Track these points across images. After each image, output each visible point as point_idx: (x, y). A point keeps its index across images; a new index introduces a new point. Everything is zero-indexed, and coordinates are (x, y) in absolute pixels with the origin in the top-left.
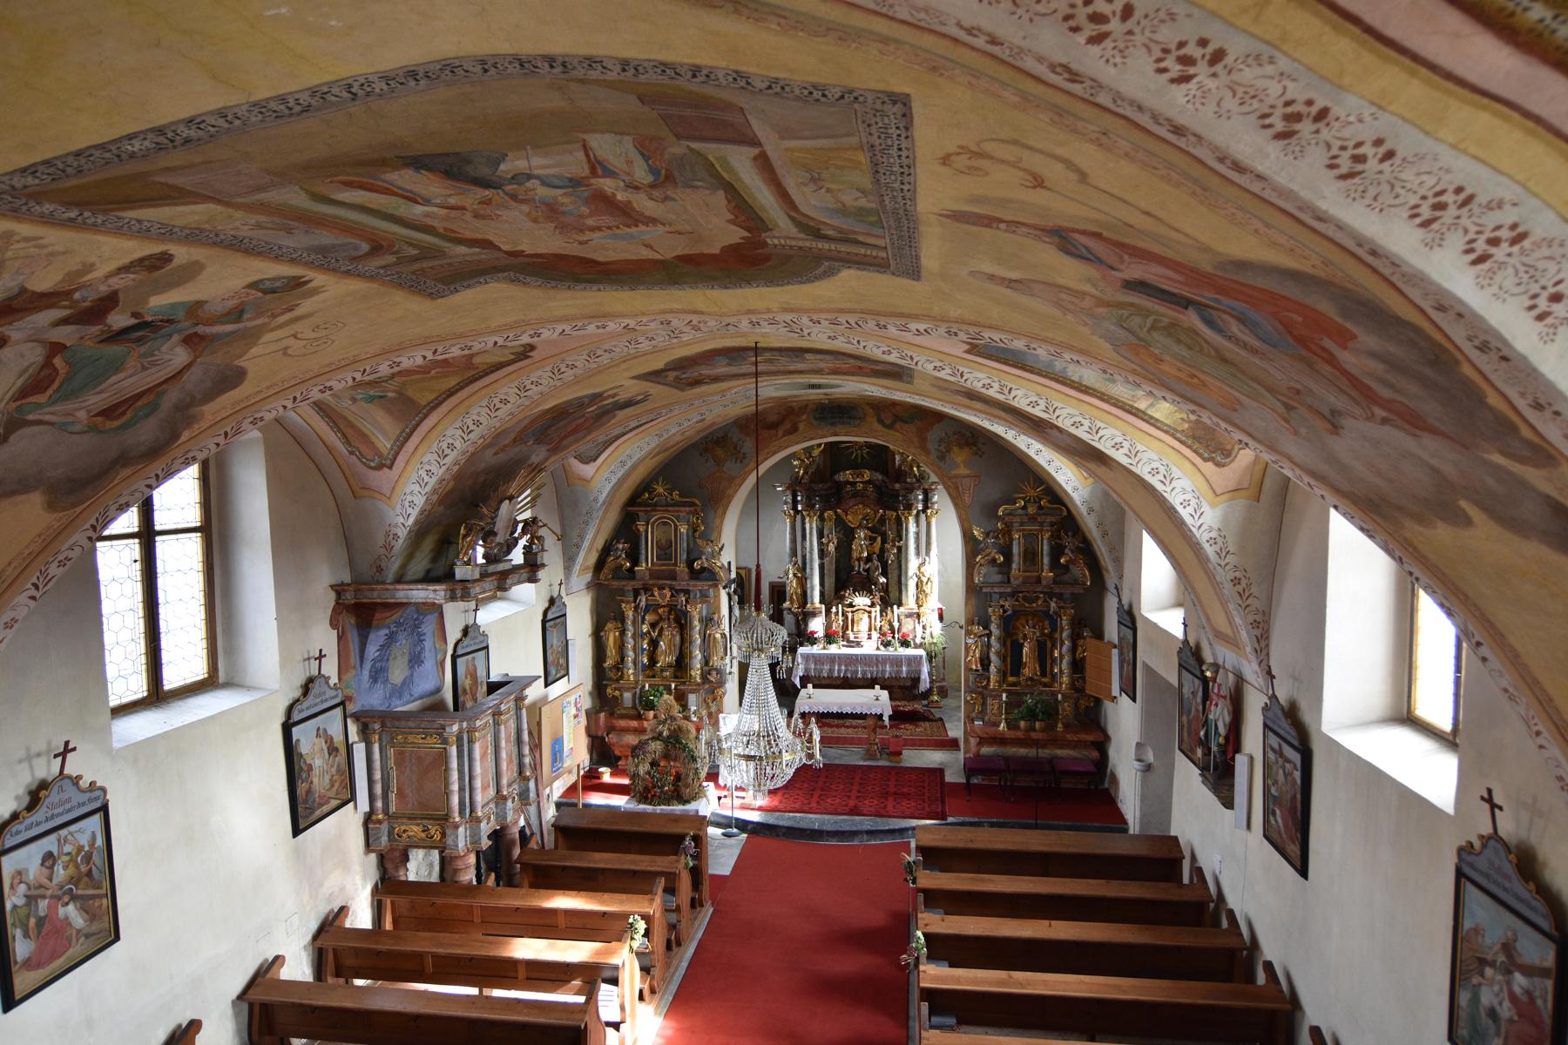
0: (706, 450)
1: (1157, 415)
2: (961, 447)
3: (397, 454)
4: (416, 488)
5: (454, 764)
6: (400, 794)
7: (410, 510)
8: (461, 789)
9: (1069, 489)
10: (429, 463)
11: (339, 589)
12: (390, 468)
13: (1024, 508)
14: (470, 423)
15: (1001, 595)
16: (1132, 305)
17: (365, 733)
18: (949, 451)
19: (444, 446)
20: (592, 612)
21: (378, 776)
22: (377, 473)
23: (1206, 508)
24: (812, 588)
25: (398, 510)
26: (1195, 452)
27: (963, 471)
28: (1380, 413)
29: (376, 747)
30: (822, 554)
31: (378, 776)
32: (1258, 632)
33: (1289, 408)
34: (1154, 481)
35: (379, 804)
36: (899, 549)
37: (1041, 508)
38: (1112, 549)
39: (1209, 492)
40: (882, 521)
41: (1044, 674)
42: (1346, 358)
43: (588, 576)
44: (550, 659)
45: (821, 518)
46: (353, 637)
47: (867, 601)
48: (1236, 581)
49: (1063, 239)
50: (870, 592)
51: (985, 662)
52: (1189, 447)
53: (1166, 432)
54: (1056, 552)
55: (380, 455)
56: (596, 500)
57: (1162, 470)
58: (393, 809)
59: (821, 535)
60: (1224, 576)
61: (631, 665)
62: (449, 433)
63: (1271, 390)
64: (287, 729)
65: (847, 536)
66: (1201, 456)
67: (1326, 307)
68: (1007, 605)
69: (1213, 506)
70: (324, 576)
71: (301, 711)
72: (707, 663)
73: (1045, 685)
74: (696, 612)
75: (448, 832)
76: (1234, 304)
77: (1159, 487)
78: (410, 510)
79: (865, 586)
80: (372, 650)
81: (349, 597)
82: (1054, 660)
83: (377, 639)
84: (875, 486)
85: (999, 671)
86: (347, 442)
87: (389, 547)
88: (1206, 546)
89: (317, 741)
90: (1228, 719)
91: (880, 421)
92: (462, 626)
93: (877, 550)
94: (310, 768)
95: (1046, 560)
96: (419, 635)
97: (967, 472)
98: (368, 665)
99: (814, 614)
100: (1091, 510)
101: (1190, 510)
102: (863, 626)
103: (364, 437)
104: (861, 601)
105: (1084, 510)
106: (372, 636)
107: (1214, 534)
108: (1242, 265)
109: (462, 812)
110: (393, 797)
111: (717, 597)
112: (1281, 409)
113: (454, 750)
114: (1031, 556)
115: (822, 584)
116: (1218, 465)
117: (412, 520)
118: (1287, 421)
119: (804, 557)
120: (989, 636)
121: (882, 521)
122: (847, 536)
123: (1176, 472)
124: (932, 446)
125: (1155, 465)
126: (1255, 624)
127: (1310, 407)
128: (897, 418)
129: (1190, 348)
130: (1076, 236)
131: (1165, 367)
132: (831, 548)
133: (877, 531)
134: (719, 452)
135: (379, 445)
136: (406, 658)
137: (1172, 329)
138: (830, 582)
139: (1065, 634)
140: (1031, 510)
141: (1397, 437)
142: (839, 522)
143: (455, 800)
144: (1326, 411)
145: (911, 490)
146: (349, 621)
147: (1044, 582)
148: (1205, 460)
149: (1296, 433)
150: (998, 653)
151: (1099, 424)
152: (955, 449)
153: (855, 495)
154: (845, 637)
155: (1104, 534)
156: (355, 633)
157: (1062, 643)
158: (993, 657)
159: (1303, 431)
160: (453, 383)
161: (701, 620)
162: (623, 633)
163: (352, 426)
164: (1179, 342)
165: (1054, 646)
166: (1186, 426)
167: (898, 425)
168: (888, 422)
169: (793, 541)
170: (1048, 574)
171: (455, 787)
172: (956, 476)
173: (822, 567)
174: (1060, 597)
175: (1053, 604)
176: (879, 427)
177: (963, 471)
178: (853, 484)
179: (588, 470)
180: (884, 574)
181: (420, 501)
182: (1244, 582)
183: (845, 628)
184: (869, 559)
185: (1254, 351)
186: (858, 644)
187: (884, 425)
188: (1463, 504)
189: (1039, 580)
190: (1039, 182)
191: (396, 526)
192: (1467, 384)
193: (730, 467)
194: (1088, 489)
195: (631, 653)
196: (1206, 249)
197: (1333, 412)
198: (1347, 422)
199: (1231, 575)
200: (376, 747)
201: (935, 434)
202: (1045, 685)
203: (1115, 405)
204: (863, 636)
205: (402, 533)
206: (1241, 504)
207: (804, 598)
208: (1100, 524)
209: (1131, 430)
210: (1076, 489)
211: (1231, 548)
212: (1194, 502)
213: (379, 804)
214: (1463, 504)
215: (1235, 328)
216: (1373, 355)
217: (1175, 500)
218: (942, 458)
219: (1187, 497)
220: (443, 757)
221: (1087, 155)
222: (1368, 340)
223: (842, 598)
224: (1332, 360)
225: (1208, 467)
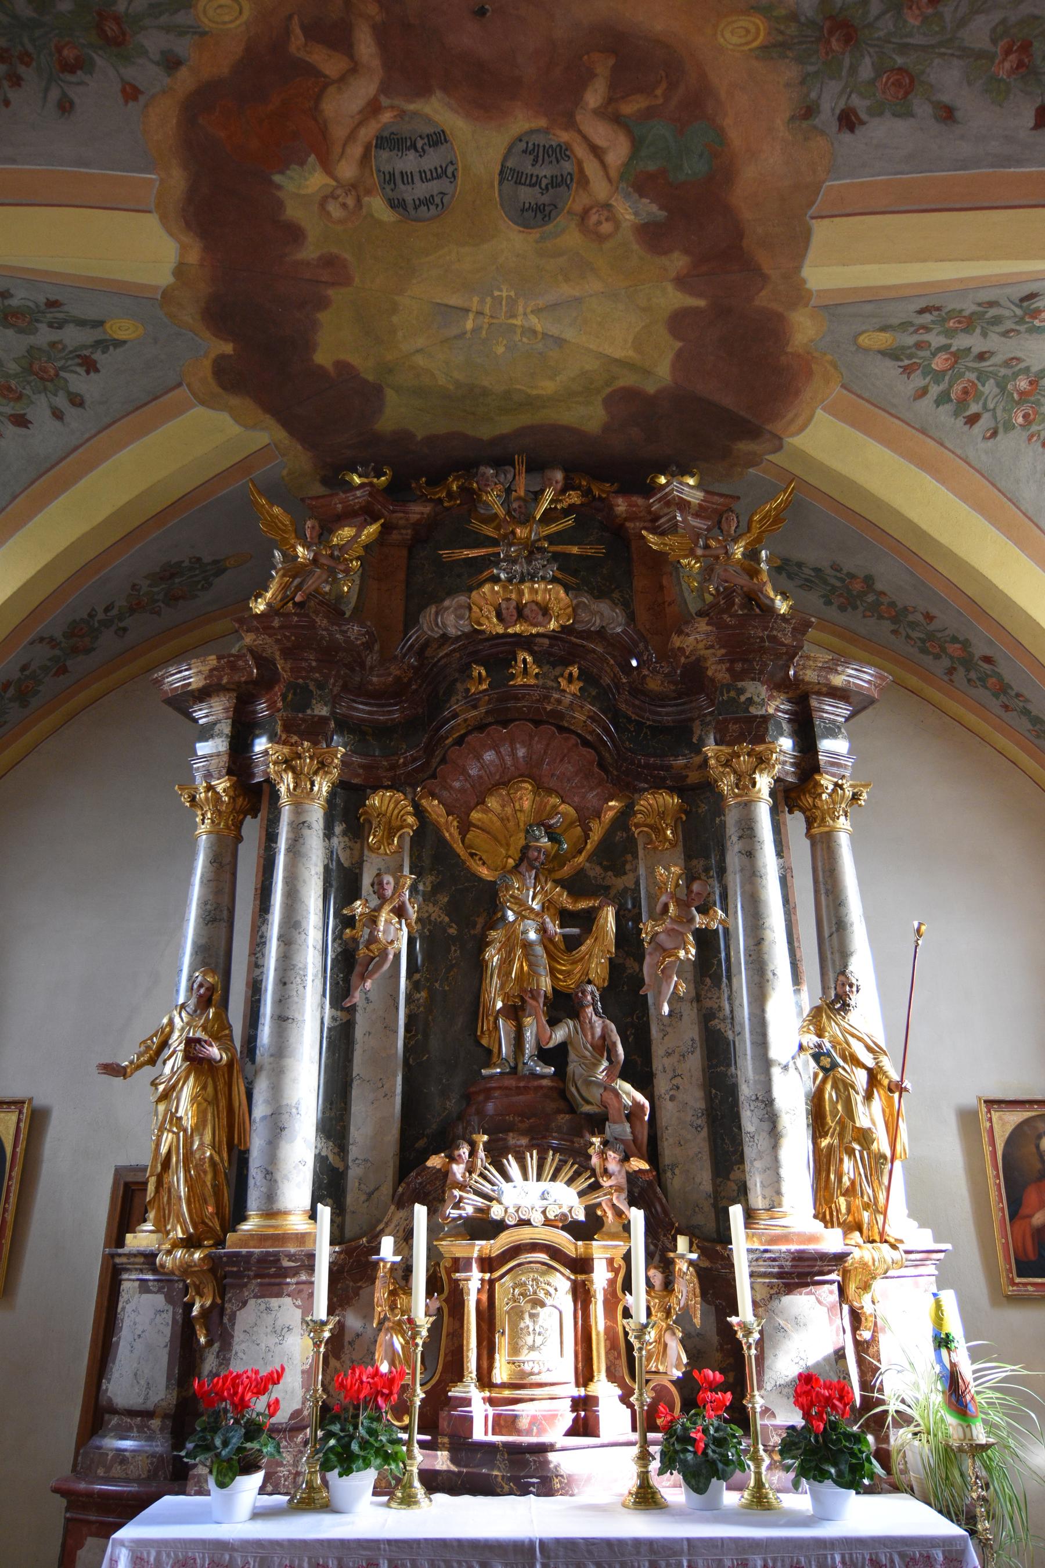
24: (277, 1128)
30: (349, 964)
40: (618, 850)
45: (347, 811)
47: (565, 1198)
50: (575, 1163)
59: (343, 884)
65: (461, 914)
79: (554, 1124)
93: (598, 968)
99: (273, 1270)
102: (546, 1344)
104: (532, 1196)
115: (334, 1125)
132: (396, 936)
133: (600, 873)
138: (376, 1118)
142: (433, 856)
153: (506, 713)
154: (441, 1420)
169: (219, 915)
173: (340, 1044)
178: (498, 653)
180: (638, 1070)
183: (445, 1360)
184: (563, 1006)
186: (522, 1469)
204: (546, 1417)
207: (232, 1178)
223: (436, 1192)
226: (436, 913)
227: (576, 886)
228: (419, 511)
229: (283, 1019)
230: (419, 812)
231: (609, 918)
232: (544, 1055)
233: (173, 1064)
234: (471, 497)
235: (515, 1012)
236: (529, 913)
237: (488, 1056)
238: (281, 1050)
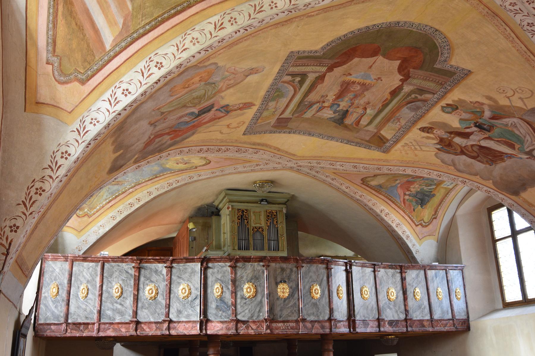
16: (211, 99)
28: (152, 137)
33: (163, 113)
42: (167, 137)
49: (227, 110)
63: (170, 112)
67: (178, 139)
76: (190, 125)
108: (193, 134)
112: (163, 110)
118: (158, 109)
127: (159, 120)
129: (194, 99)
130: (223, 115)
131: (197, 79)
137: (200, 98)
141: (145, 138)
144: (156, 124)
149: (154, 110)
159: (153, 113)
164: (197, 98)
185: (180, 117)
188: (122, 151)
190: (228, 126)
192: (155, 153)
196: (200, 132)
197: (156, 126)
198: (152, 128)
214: (122, 151)
215: (187, 119)
216: (166, 142)
221: (219, 136)
222: (170, 142)
224: (168, 134)
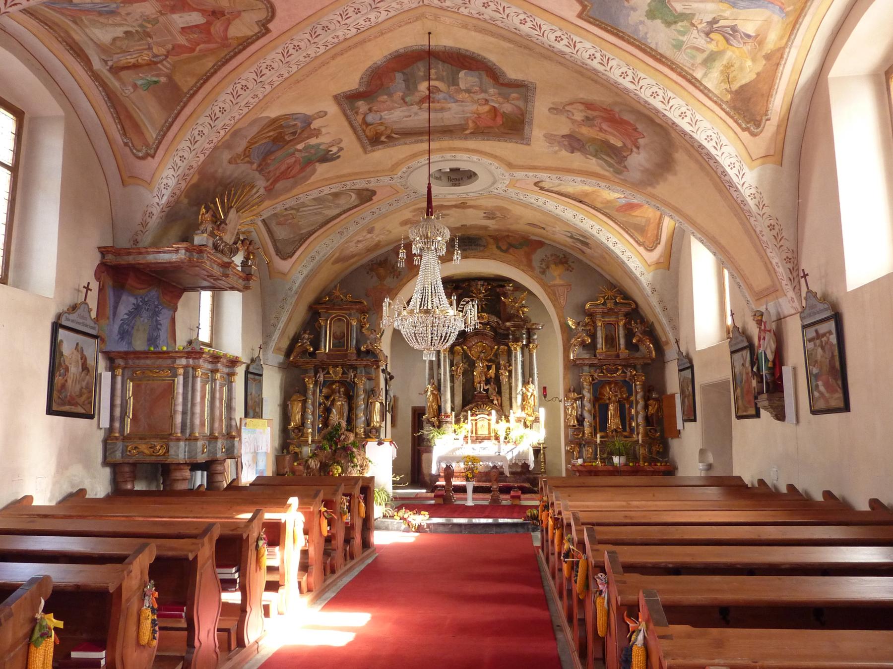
0: (372, 270)
1: (709, 85)
2: (556, 264)
3: (160, 143)
4: (171, 172)
5: (180, 390)
6: (135, 418)
7: (164, 191)
8: (184, 413)
9: (638, 274)
10: (183, 150)
11: (103, 251)
12: (153, 157)
13: (604, 304)
14: (217, 109)
15: (591, 365)
17: (112, 368)
18: (548, 267)
19: (196, 132)
20: (281, 387)
21: (118, 401)
22: (143, 162)
23: (746, 170)
25: (155, 192)
26: (736, 122)
27: (558, 281)
29: (119, 379)
31: (118, 401)
32: (790, 266)
34: (709, 146)
35: (117, 425)
36: (510, 372)
37: (616, 303)
38: (670, 321)
39: (749, 160)
40: (496, 355)
41: (624, 429)
43: (281, 358)
44: (250, 402)
46: (110, 293)
48: (771, 227)
51: (580, 420)
52: (732, 117)
53: (715, 102)
54: (629, 335)
55: (147, 146)
56: (290, 289)
57: (714, 137)
58: (128, 430)
60: (761, 225)
61: (310, 426)
62: (200, 121)
64: (56, 326)
66: (739, 125)
68: (596, 375)
69: (751, 168)
70: (94, 238)
71: (68, 320)
72: (368, 425)
73: (626, 437)
74: (362, 385)
75: (172, 444)
77: (713, 152)
78: (164, 191)
80: (123, 310)
81: (109, 258)
82: (632, 418)
83: (127, 303)
84: (491, 327)
85: (591, 425)
86: (125, 134)
87: (144, 224)
88: (749, 199)
89: (75, 352)
90: (774, 346)
91: (499, 248)
92: (188, 339)
94: (67, 369)
95: (622, 341)
96: (158, 323)
97: (562, 282)
98: (118, 322)
100: (654, 290)
101: (735, 171)
103: (136, 126)
105: (648, 290)
106: (124, 298)
107: (753, 191)
109: (183, 431)
110: (128, 421)
111: (378, 377)
113: (181, 378)
114: (611, 340)
115: (453, 401)
116: (753, 135)
117: (165, 198)
119: (439, 381)
120: (582, 399)
121: (496, 355)
122: (472, 365)
123: (724, 140)
124: (536, 263)
125: (709, 133)
126: (788, 260)
128: (511, 246)
133: (494, 361)
134: (382, 271)
135: (147, 135)
136: (146, 336)
138: (459, 400)
139: (639, 396)
140: (610, 305)
142: (466, 356)
143: (179, 419)
145: (518, 327)
146: (109, 283)
147: (621, 357)
148: (744, 130)
150: (590, 412)
151: (670, 94)
152: (553, 266)
155: (665, 309)
156: (111, 294)
157: (637, 403)
158: (586, 414)
160: (210, 65)
161: (365, 391)
162: (304, 402)
163: (130, 117)
165: (631, 407)
166: (729, 96)
167: (511, 250)
168: (504, 248)
170: (624, 352)
171: (180, 408)
172: (554, 286)
174: (634, 367)
175: (629, 373)
176: (498, 252)
177: (558, 281)
179: (284, 265)
181: (172, 182)
182: (777, 228)
187: (502, 251)
189: (618, 356)
191: (152, 206)
193: (389, 281)
194: (651, 274)
195: (310, 416)
199: (768, 223)
200: (119, 379)
201: (538, 256)
202: (626, 437)
203: (680, 74)
205: (156, 211)
206: (770, 167)
208: (661, 301)
209: (692, 101)
210: (643, 274)
211: (766, 202)
212: (737, 164)
213: (117, 425)
217: (725, 162)
218: (543, 272)
219: (733, 160)
220: (171, 388)
225: (745, 135)
226: (466, 366)
227: (489, 361)
228: (460, 291)
229: (445, 387)
230: (463, 349)
231: (494, 366)
232: (484, 390)
233: (429, 393)
234: (469, 286)
235: (480, 383)
236: (480, 365)
237: (475, 389)
238: (445, 391)
